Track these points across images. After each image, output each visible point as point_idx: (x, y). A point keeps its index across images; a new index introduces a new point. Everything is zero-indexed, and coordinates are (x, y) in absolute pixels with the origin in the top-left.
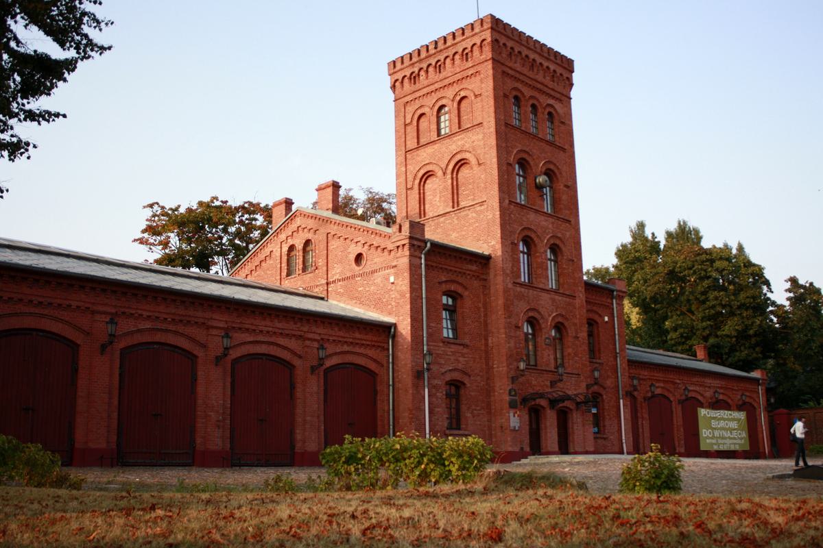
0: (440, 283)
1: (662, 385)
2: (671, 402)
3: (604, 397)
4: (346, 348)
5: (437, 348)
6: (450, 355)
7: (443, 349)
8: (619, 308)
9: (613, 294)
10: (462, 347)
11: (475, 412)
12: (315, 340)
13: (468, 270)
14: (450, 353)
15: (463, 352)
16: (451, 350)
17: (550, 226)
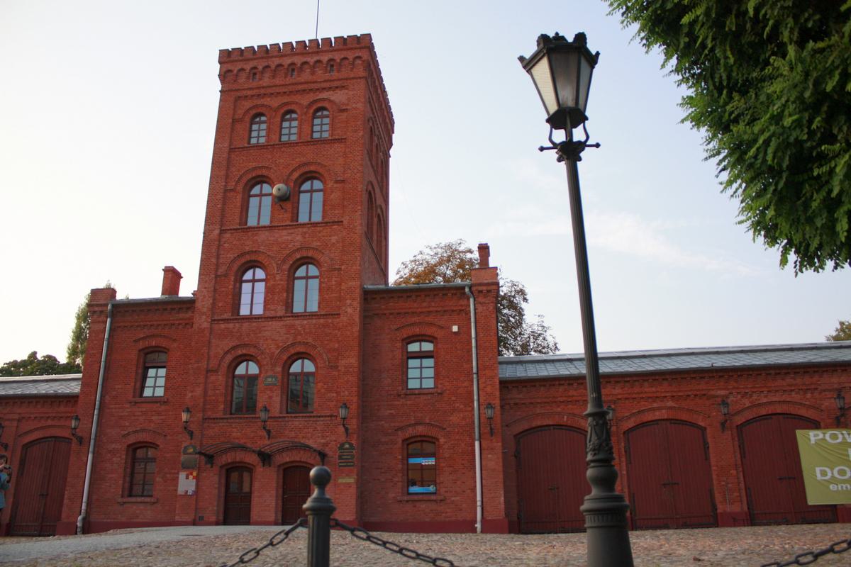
0: (136, 341)
1: (670, 404)
2: (703, 429)
3: (442, 440)
4: (50, 422)
5: (121, 410)
6: (138, 416)
7: (129, 410)
8: (480, 308)
9: (464, 293)
10: (159, 404)
11: (168, 476)
12: (14, 420)
13: (177, 320)
14: (140, 414)
15: (160, 409)
16: (140, 410)
17: (299, 238)
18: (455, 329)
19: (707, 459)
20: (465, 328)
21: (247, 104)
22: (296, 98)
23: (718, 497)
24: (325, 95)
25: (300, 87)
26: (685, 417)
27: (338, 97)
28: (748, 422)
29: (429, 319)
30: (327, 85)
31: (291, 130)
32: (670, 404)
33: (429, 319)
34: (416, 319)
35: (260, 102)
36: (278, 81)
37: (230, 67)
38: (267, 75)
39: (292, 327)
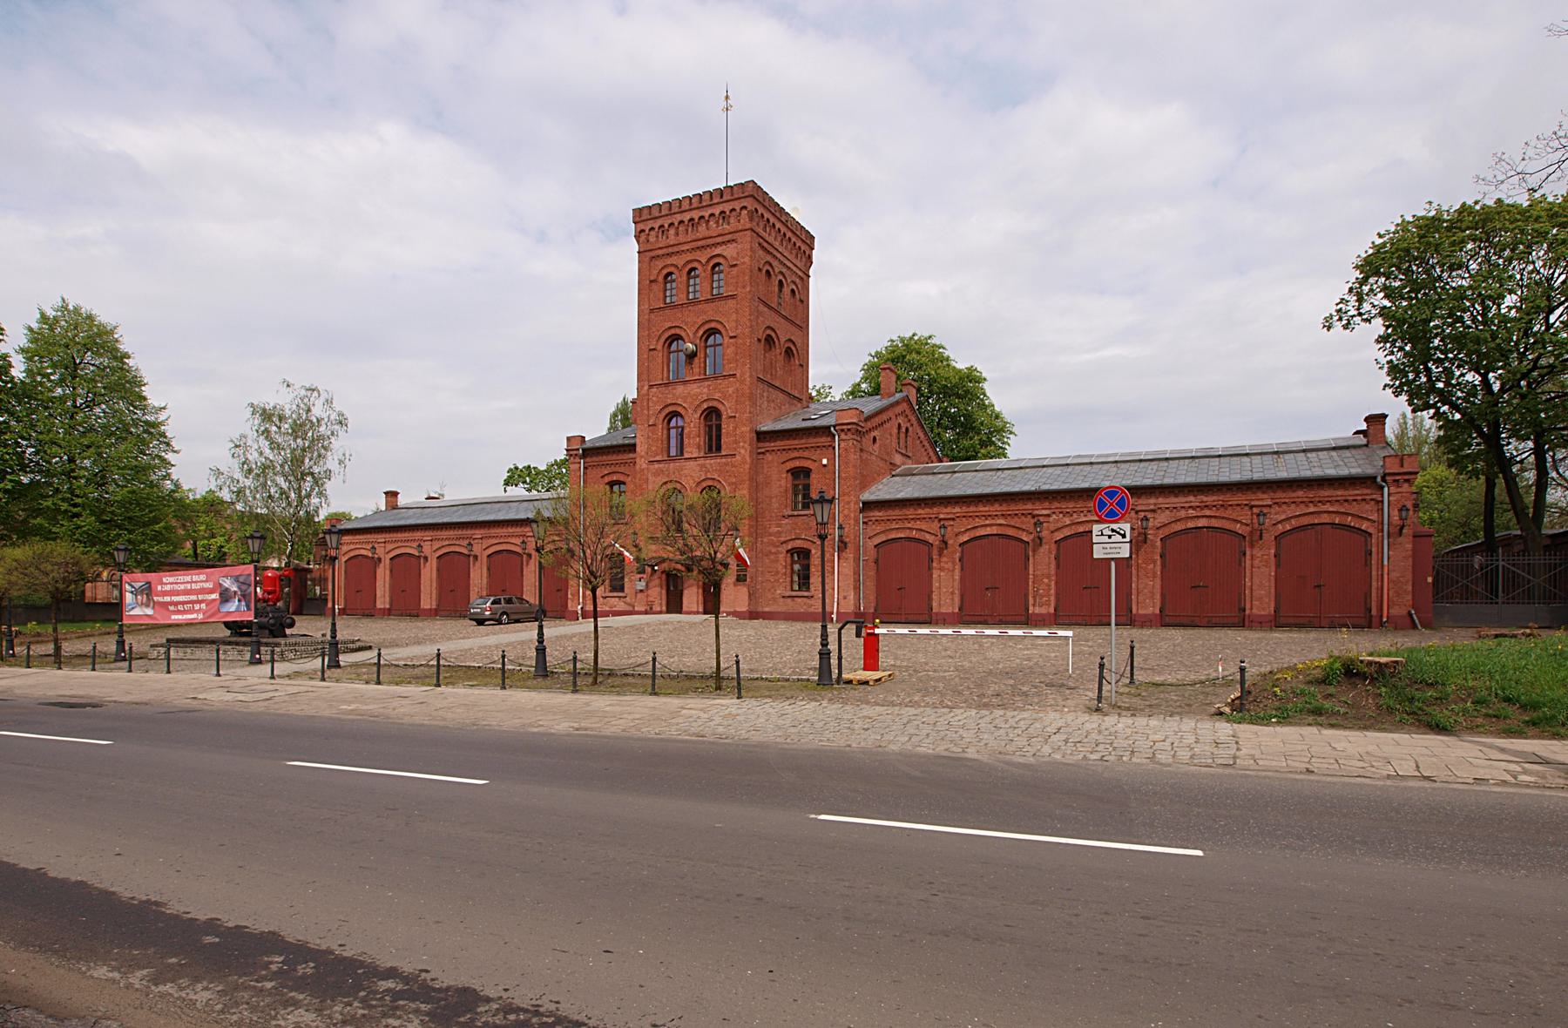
1: (1002, 521)
18: (825, 461)
19: (1026, 568)
20: (832, 460)
21: (660, 264)
22: (697, 255)
23: (1031, 601)
24: (718, 251)
25: (700, 243)
26: (1010, 532)
27: (729, 251)
28: (1065, 538)
29: (806, 454)
30: (719, 240)
31: (700, 287)
32: (1002, 521)
33: (806, 454)
34: (796, 454)
35: (669, 261)
36: (682, 239)
37: (641, 226)
38: (672, 231)
39: (702, 466)
